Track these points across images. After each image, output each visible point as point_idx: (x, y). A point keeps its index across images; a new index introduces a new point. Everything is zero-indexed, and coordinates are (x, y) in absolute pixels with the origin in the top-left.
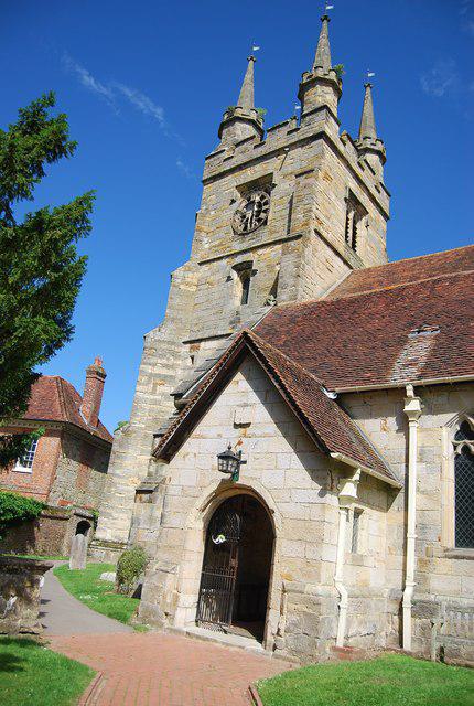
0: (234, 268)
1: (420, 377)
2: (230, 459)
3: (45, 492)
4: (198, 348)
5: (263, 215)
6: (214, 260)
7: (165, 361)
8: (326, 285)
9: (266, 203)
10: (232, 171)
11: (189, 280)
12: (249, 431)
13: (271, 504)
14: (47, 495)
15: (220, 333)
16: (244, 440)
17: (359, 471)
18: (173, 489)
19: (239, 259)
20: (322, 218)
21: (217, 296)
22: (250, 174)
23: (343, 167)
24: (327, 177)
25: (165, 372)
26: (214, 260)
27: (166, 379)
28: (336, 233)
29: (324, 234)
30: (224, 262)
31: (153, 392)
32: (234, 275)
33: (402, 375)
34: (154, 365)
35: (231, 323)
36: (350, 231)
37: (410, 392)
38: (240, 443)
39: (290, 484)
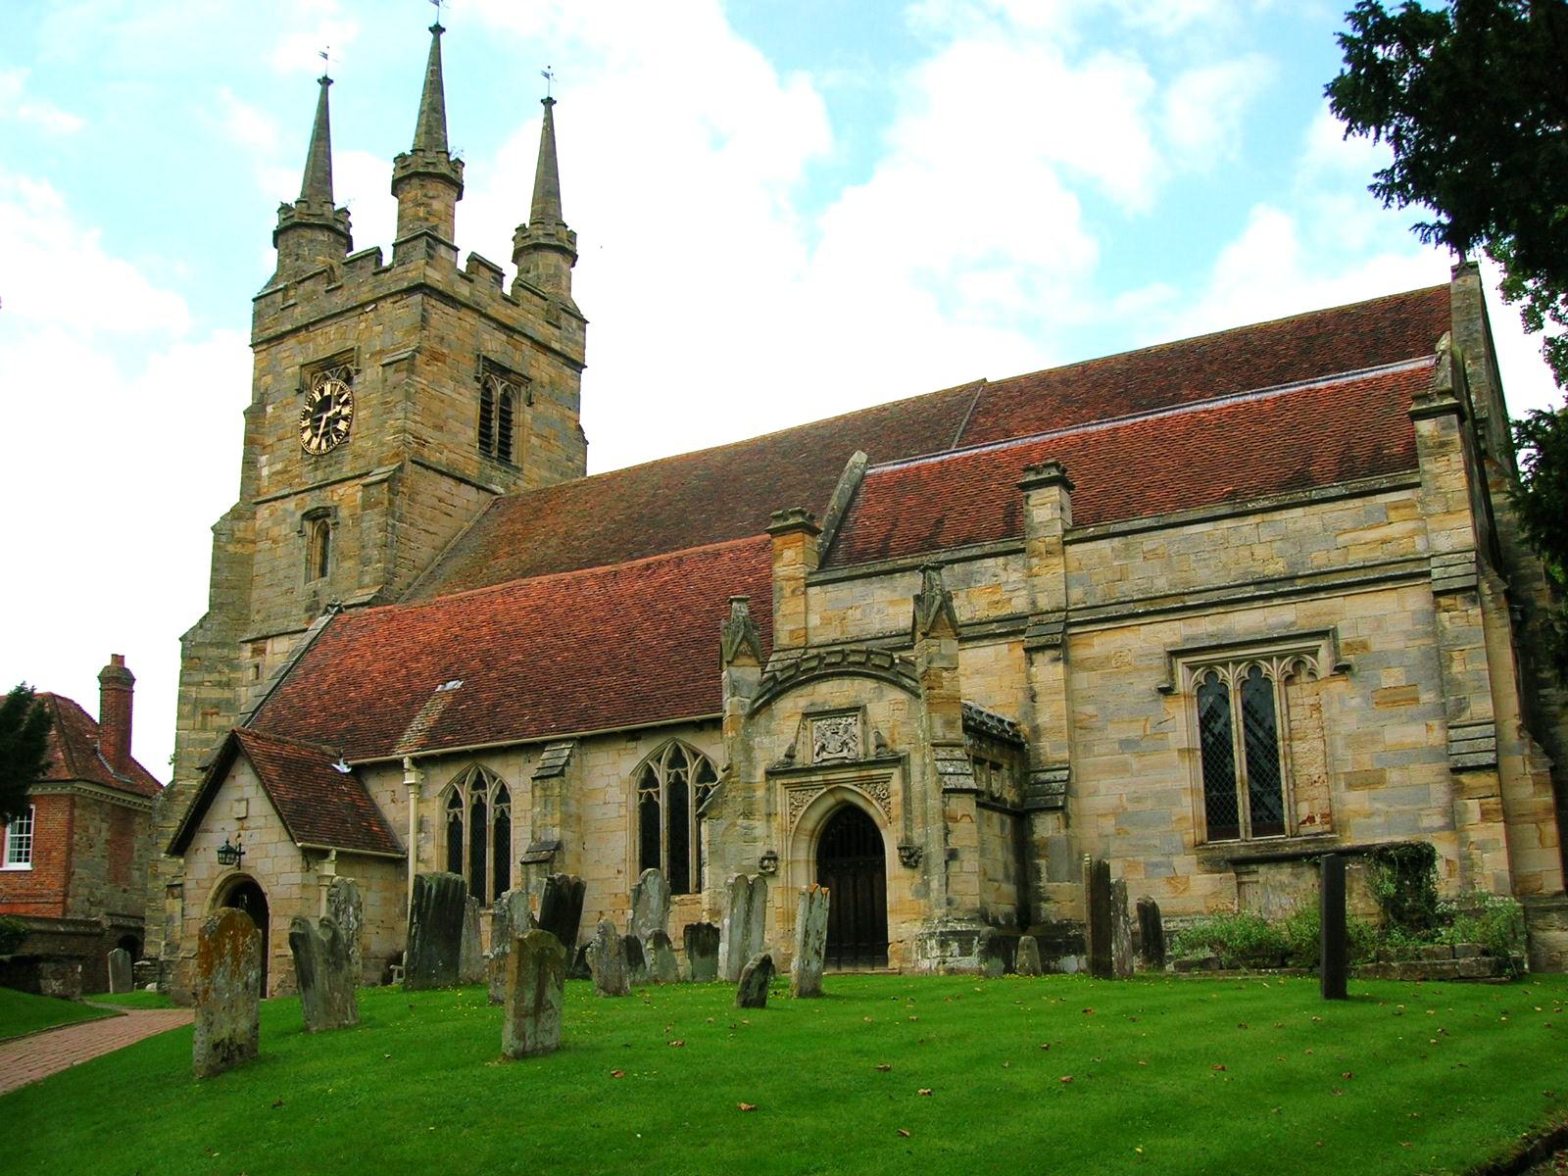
0: (306, 516)
1: (423, 747)
2: (230, 853)
3: (60, 899)
4: (263, 651)
5: (342, 426)
6: (276, 499)
7: (215, 677)
8: (439, 541)
9: (346, 403)
10: (295, 331)
11: (238, 534)
12: (246, 824)
13: (264, 889)
14: (64, 902)
15: (294, 627)
16: (242, 832)
17: (334, 853)
18: (190, 885)
19: (311, 502)
20: (427, 433)
21: (284, 562)
22: (326, 342)
23: (471, 319)
24: (436, 357)
25: (217, 694)
26: (276, 499)
27: (230, 705)
28: (461, 443)
29: (433, 457)
30: (291, 504)
31: (204, 728)
32: (308, 526)
33: (404, 753)
34: (200, 684)
35: (307, 610)
36: (495, 424)
37: (407, 763)
38: (239, 836)
39: (277, 870)
